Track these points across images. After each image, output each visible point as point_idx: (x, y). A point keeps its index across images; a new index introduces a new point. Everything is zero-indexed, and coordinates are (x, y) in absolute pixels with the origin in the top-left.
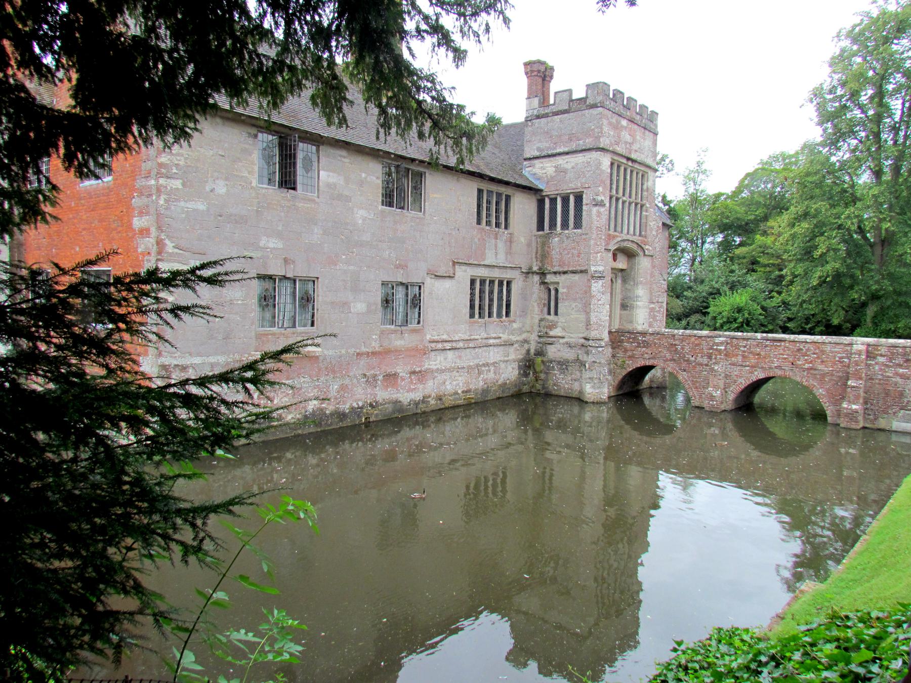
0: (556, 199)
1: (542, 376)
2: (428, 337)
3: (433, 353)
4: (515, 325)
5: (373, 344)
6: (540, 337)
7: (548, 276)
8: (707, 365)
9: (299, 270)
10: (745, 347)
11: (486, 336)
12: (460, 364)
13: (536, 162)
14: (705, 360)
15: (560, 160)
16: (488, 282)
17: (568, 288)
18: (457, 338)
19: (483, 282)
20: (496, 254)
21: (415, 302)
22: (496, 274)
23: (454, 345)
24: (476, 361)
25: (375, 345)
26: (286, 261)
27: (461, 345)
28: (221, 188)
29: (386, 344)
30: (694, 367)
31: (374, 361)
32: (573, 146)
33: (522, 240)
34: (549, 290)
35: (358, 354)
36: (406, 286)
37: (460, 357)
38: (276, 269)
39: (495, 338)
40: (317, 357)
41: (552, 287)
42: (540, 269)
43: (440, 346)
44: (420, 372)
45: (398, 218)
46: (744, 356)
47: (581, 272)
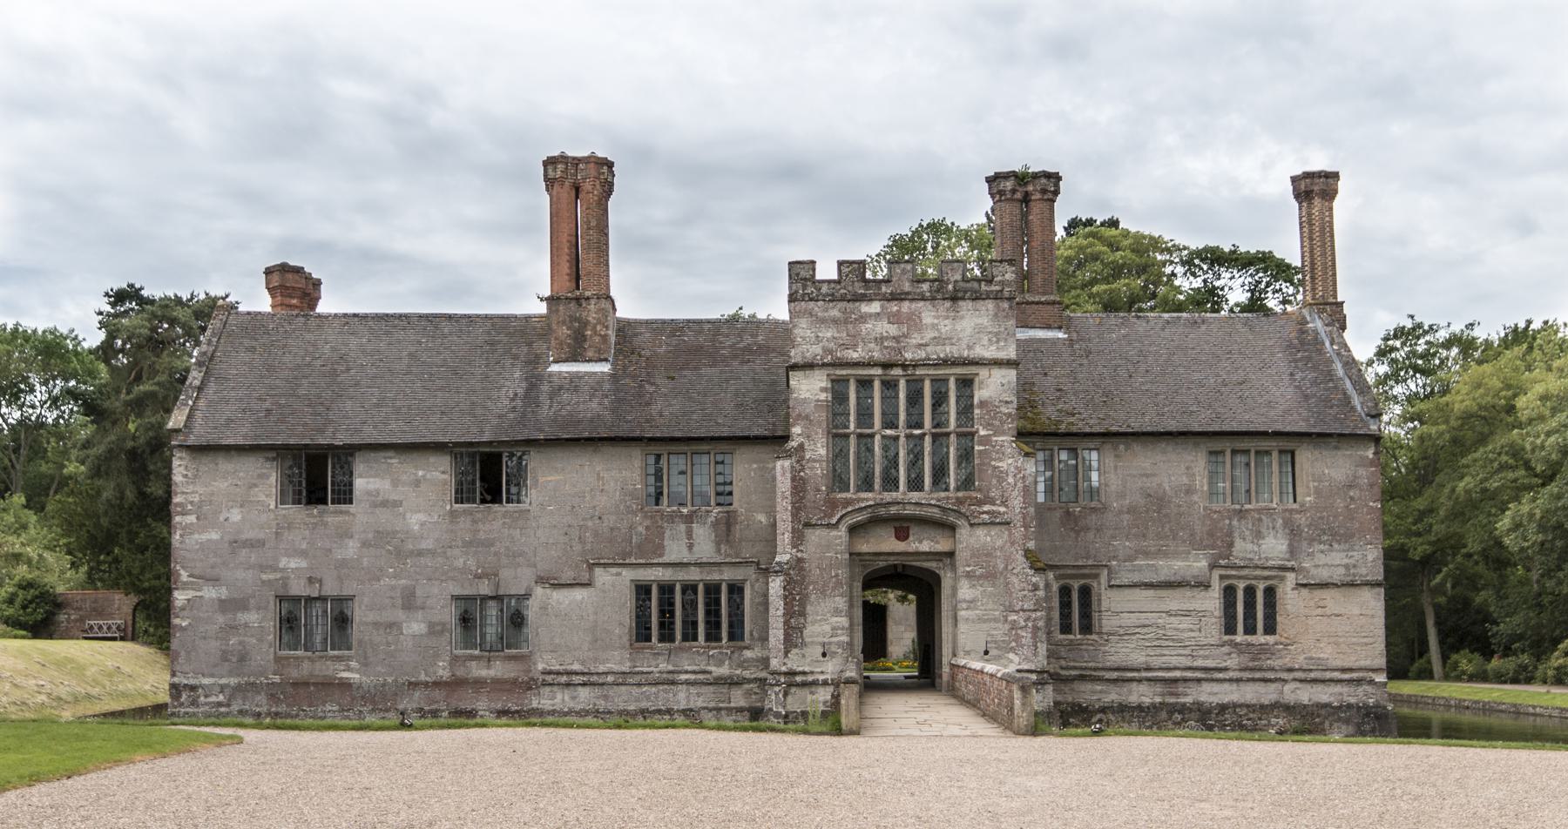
2: (540, 667)
3: (548, 689)
4: (748, 654)
5: (441, 672)
9: (330, 589)
11: (670, 668)
12: (602, 705)
16: (678, 588)
18: (602, 669)
19: (666, 589)
20: (690, 547)
21: (517, 620)
22: (694, 575)
23: (594, 679)
24: (644, 705)
25: (443, 671)
26: (311, 580)
27: (610, 679)
28: (236, 516)
29: (460, 672)
31: (437, 694)
33: (762, 518)
35: (410, 683)
36: (498, 598)
37: (606, 697)
38: (298, 588)
39: (694, 672)
40: (350, 685)
43: (564, 679)
44: (517, 712)
45: (479, 516)
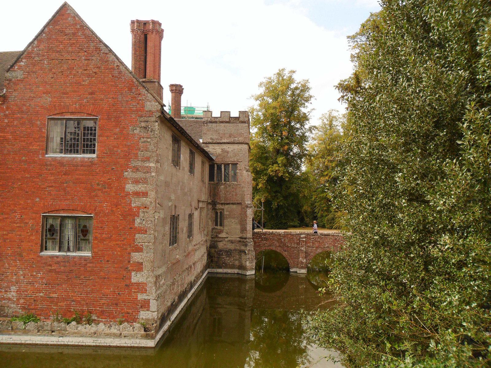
0: (221, 165)
1: (216, 259)
6: (212, 238)
7: (218, 206)
8: (296, 248)
10: (313, 239)
13: (210, 145)
14: (296, 245)
15: (225, 147)
17: (229, 211)
30: (291, 249)
32: (232, 140)
34: (217, 213)
41: (219, 211)
42: (212, 201)
46: (313, 243)
47: (238, 204)
